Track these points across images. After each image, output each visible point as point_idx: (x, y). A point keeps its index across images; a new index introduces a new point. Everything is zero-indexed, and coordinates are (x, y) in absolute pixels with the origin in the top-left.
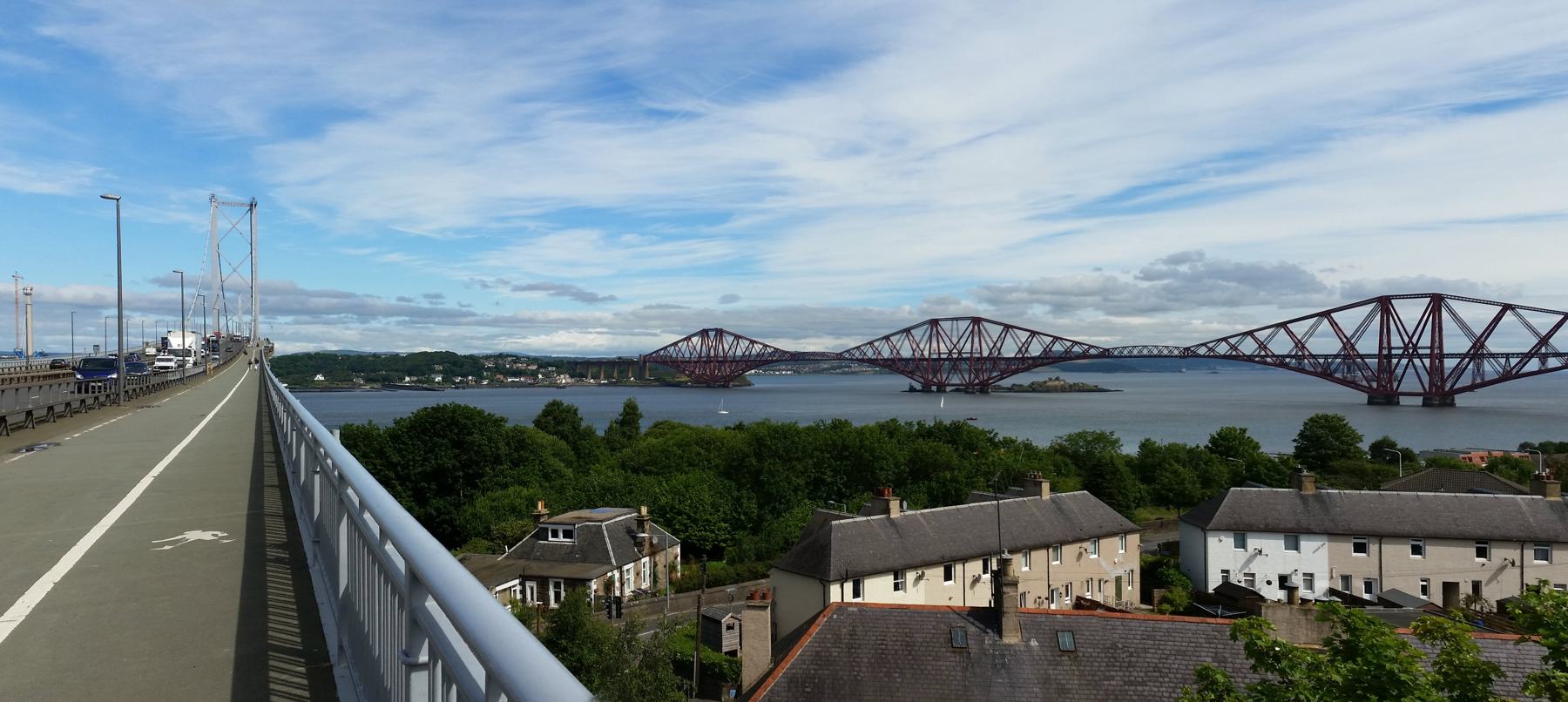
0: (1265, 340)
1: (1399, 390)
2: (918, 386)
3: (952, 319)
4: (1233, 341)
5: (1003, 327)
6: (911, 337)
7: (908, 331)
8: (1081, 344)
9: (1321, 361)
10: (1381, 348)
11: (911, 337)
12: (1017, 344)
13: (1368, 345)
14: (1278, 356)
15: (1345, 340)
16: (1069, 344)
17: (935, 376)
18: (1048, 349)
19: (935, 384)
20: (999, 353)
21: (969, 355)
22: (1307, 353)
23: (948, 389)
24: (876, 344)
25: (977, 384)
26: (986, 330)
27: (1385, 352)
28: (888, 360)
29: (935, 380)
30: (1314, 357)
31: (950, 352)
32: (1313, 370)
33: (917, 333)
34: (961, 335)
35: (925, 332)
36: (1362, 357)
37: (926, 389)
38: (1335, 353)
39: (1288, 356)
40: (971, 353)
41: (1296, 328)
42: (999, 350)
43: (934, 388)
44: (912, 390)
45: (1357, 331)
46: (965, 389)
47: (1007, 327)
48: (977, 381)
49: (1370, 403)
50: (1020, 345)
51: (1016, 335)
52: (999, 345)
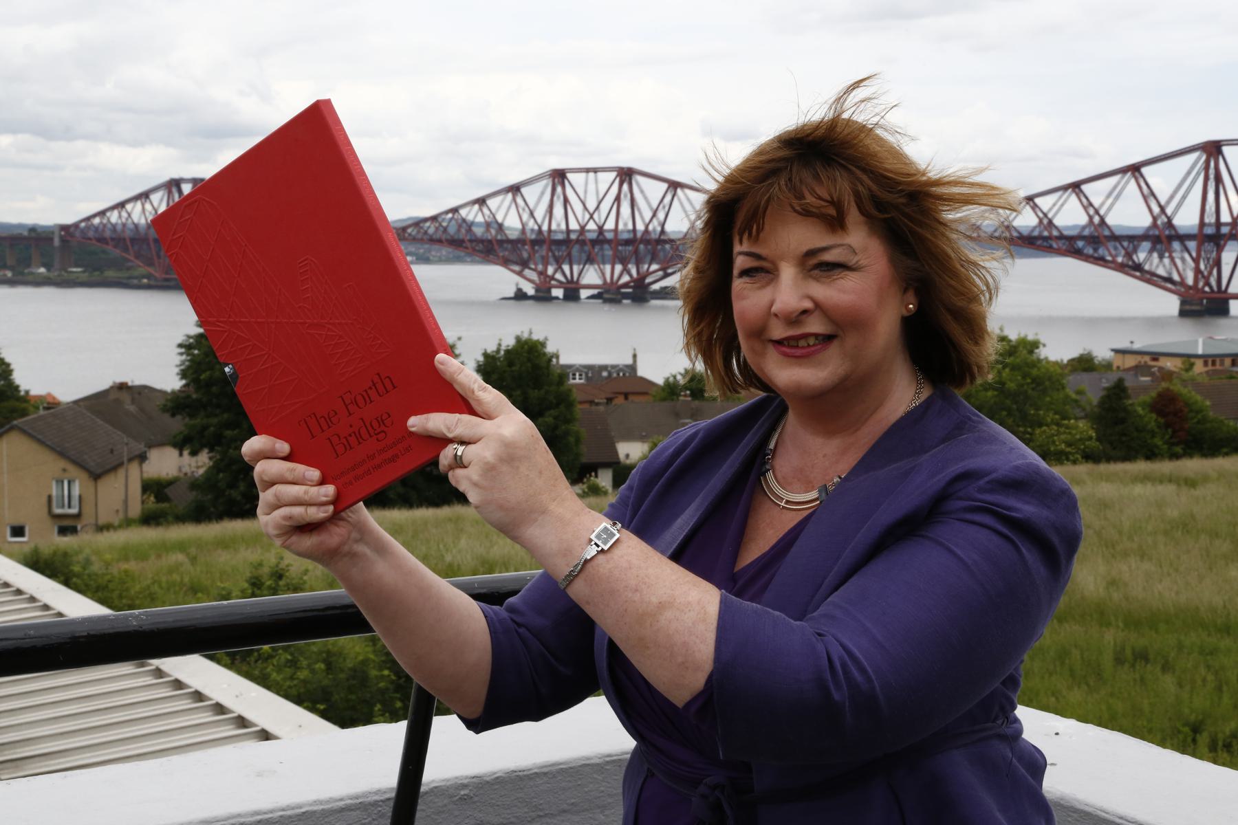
0: (1050, 209)
1: (1232, 290)
2: (529, 290)
3: (587, 170)
6: (519, 200)
7: (515, 189)
9: (1125, 244)
10: (1202, 224)
11: (519, 200)
13: (1187, 218)
15: (1156, 210)
17: (559, 268)
19: (560, 285)
20: (663, 232)
21: (631, 236)
23: (584, 294)
24: (463, 212)
25: (626, 285)
26: (642, 192)
27: (1209, 231)
28: (482, 241)
29: (559, 276)
31: (583, 229)
33: (530, 193)
34: (601, 196)
35: (543, 193)
36: (1183, 238)
37: (543, 296)
39: (1080, 237)
40: (616, 230)
41: (1095, 192)
42: (663, 225)
43: (558, 293)
44: (520, 296)
45: (1172, 197)
46: (610, 295)
47: (674, 186)
48: (626, 278)
49: (1183, 313)
52: (661, 215)
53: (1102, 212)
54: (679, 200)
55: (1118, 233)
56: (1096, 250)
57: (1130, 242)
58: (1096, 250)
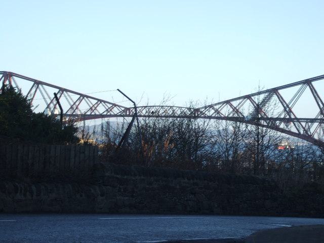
4: (235, 104)
5: (33, 83)
8: (105, 102)
9: (304, 124)
12: (46, 101)
14: (271, 119)
16: (94, 102)
18: (75, 107)
22: (293, 117)
30: (299, 120)
32: (297, 132)
38: (314, 117)
39: (277, 119)
41: (287, 94)
50: (49, 101)
51: (44, 89)
53: (290, 106)
54: (40, 91)
55: (298, 117)
56: (287, 126)
57: (307, 122)
58: (287, 126)
